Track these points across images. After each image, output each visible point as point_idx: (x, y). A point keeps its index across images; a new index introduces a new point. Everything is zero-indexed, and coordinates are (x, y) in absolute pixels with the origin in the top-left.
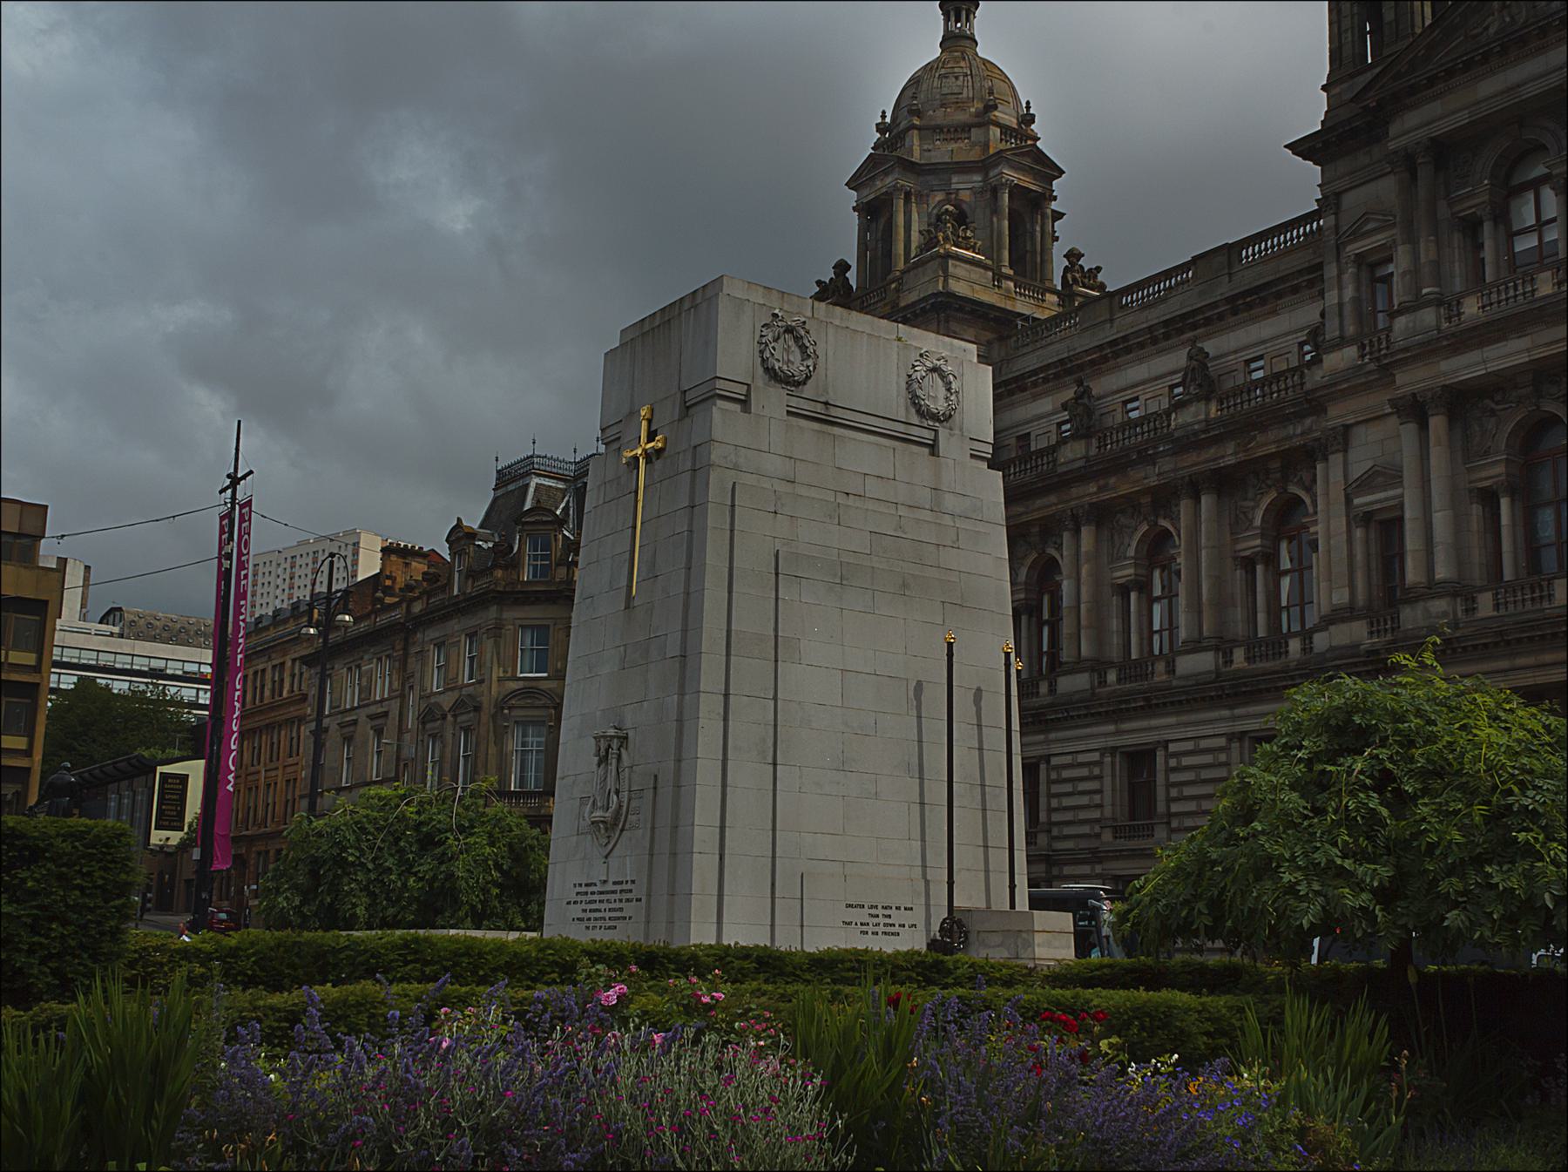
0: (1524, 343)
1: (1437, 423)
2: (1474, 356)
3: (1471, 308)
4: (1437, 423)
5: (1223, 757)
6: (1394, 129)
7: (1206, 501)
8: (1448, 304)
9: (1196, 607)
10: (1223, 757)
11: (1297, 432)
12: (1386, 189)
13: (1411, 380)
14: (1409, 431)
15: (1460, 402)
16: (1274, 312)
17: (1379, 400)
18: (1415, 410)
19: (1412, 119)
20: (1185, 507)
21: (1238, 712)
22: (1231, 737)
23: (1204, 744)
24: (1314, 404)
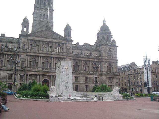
0: (35, 54)
1: (29, 57)
2: (32, 54)
3: (32, 51)
4: (29, 57)
5: (6, 75)
6: (28, 37)
7: (7, 56)
8: (31, 50)
9: (5, 63)
10: (6, 75)
11: (16, 53)
12: (26, 40)
13: (28, 54)
14: (27, 57)
15: (31, 56)
16: (13, 44)
17: (25, 54)
18: (28, 56)
19: (29, 37)
20: (4, 56)
21: (9, 72)
22: (7, 73)
23: (5, 74)
24: (19, 52)
